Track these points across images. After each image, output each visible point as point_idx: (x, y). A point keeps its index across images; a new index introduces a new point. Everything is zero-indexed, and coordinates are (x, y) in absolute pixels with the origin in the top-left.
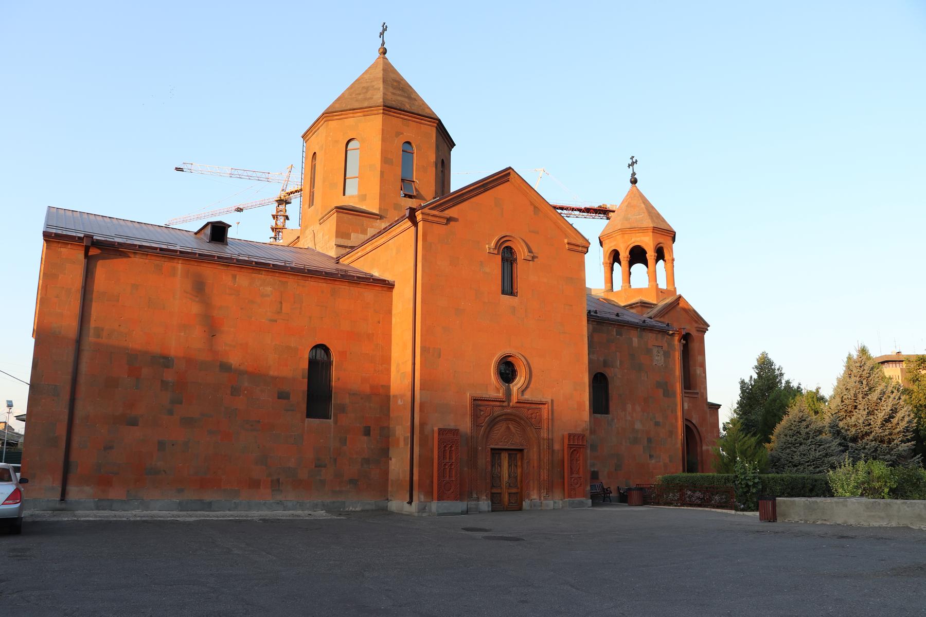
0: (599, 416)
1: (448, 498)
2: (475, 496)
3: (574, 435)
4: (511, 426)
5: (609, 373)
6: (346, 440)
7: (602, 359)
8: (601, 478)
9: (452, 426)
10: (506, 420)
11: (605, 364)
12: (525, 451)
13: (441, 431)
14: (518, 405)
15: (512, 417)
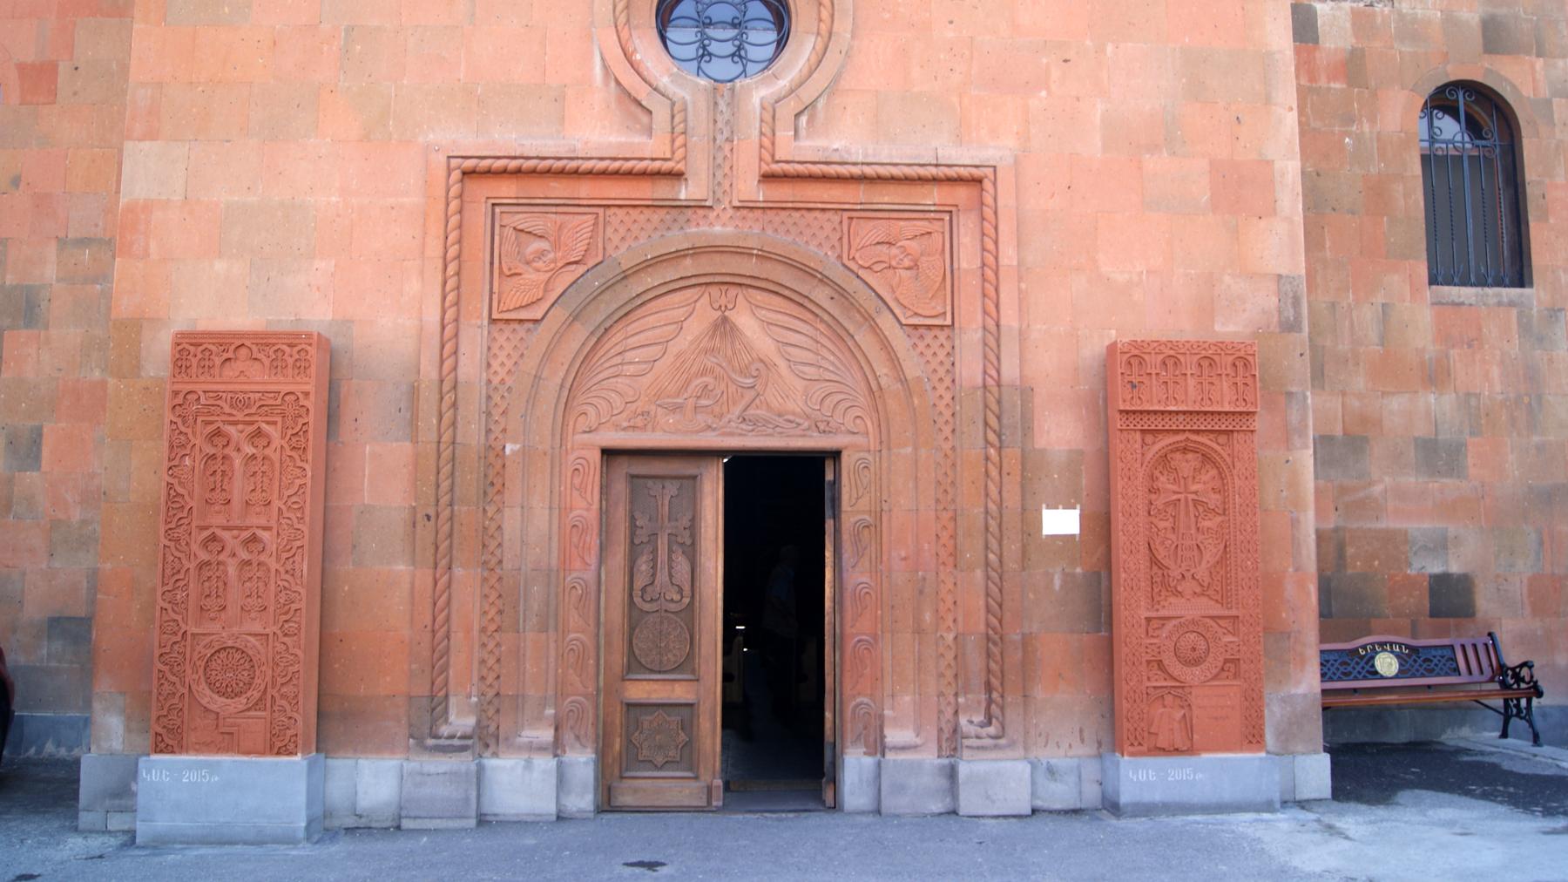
0: (1467, 293)
1: (227, 740)
2: (461, 721)
3: (1172, 357)
4: (745, 321)
5: (1518, 80)
6: (36, 438)
7: (1471, 16)
8: (1485, 603)
9: (316, 315)
10: (706, 283)
11: (1495, 37)
12: (845, 459)
13: (196, 351)
14: (784, 192)
15: (749, 267)
